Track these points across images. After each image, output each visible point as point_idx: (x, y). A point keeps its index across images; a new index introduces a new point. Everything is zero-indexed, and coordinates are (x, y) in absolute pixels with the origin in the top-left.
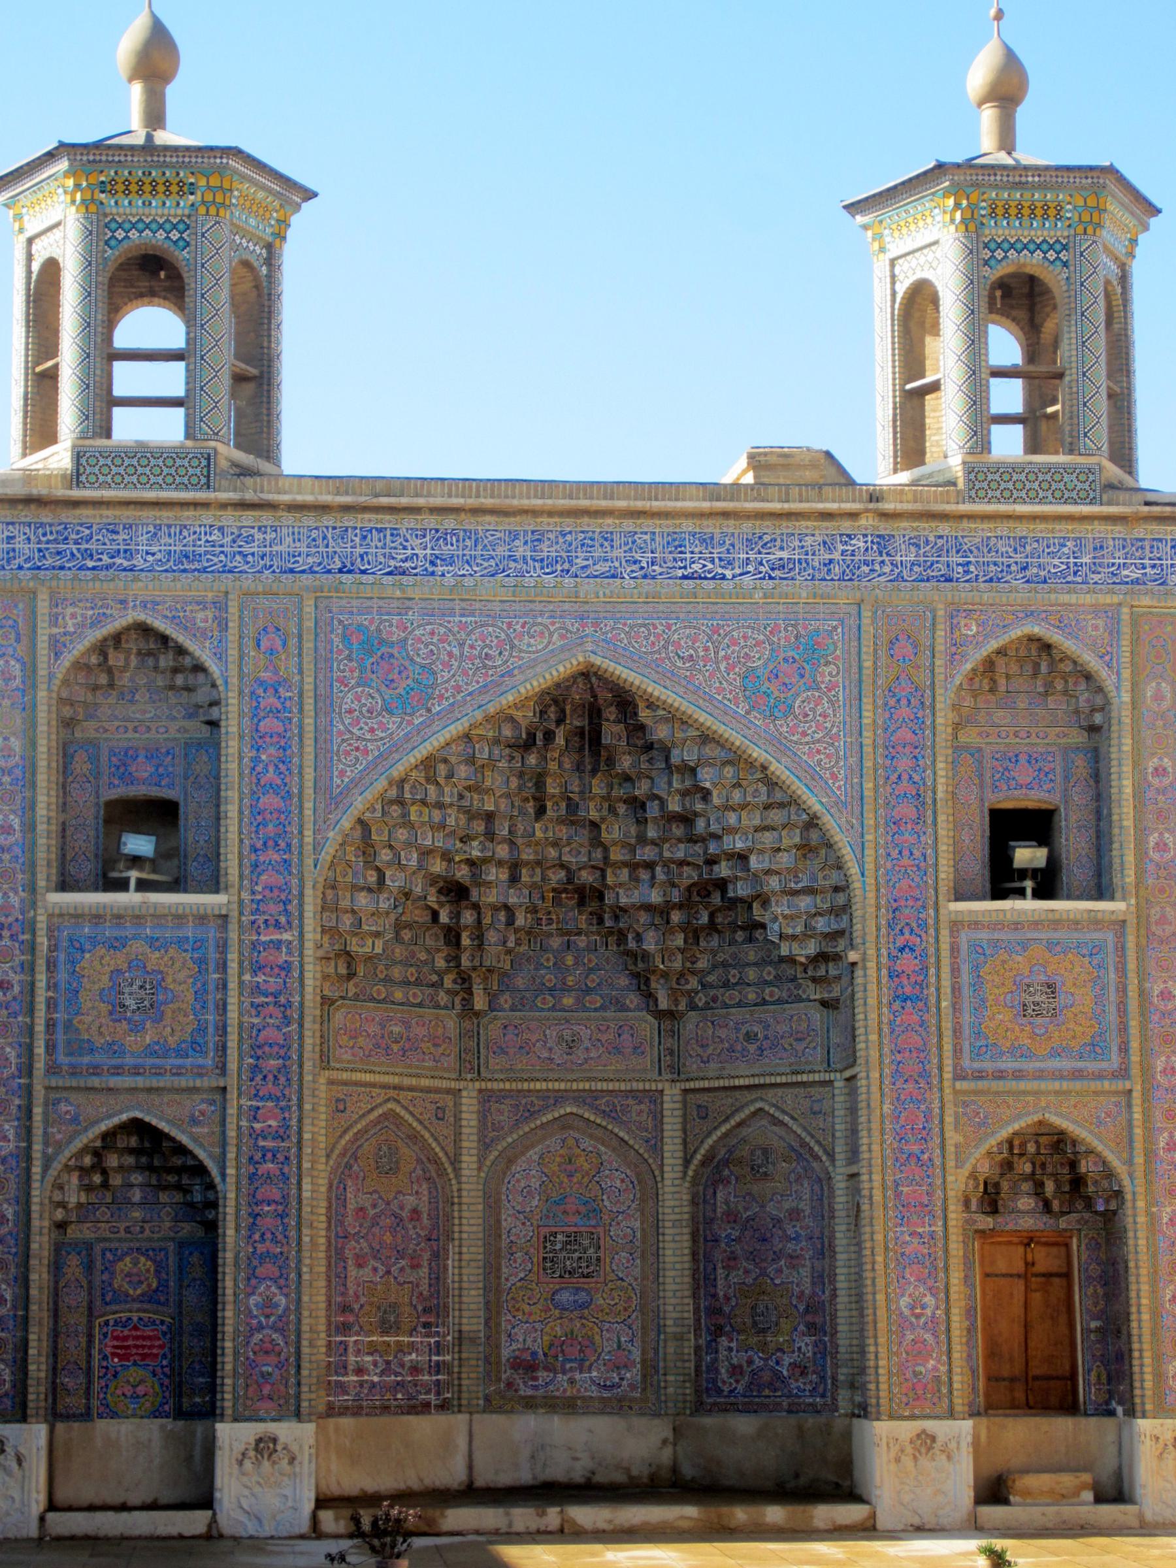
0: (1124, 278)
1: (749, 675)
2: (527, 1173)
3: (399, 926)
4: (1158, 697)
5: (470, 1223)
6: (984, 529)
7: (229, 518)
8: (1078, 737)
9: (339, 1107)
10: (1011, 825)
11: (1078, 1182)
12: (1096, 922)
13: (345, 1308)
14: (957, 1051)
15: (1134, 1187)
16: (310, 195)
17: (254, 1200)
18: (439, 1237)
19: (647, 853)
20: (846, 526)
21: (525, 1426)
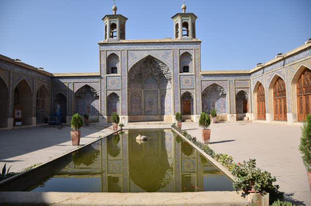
0: (194, 23)
5: (143, 100)
15: (194, 96)
16: (127, 19)
18: (140, 101)
21: (147, 116)
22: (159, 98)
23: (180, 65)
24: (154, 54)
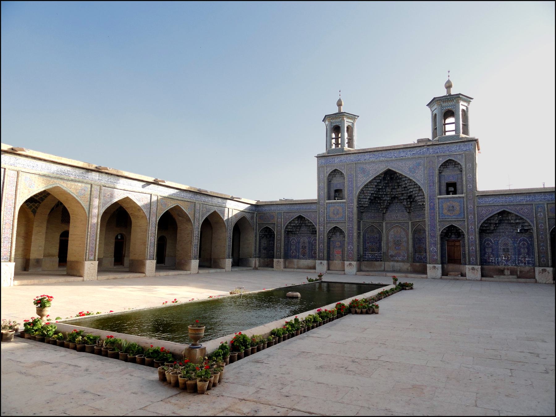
1: (410, 168)
2: (392, 232)
3: (370, 202)
4: (469, 166)
5: (384, 239)
6: (442, 146)
7: (345, 156)
8: (459, 172)
9: (365, 224)
10: (449, 185)
11: (460, 233)
12: (460, 197)
13: (366, 249)
14: (439, 216)
15: (465, 233)
17: (349, 236)
18: (380, 240)
19: (403, 192)
20: (423, 148)
21: (392, 263)
22: (410, 236)
23: (440, 181)
24: (396, 167)
